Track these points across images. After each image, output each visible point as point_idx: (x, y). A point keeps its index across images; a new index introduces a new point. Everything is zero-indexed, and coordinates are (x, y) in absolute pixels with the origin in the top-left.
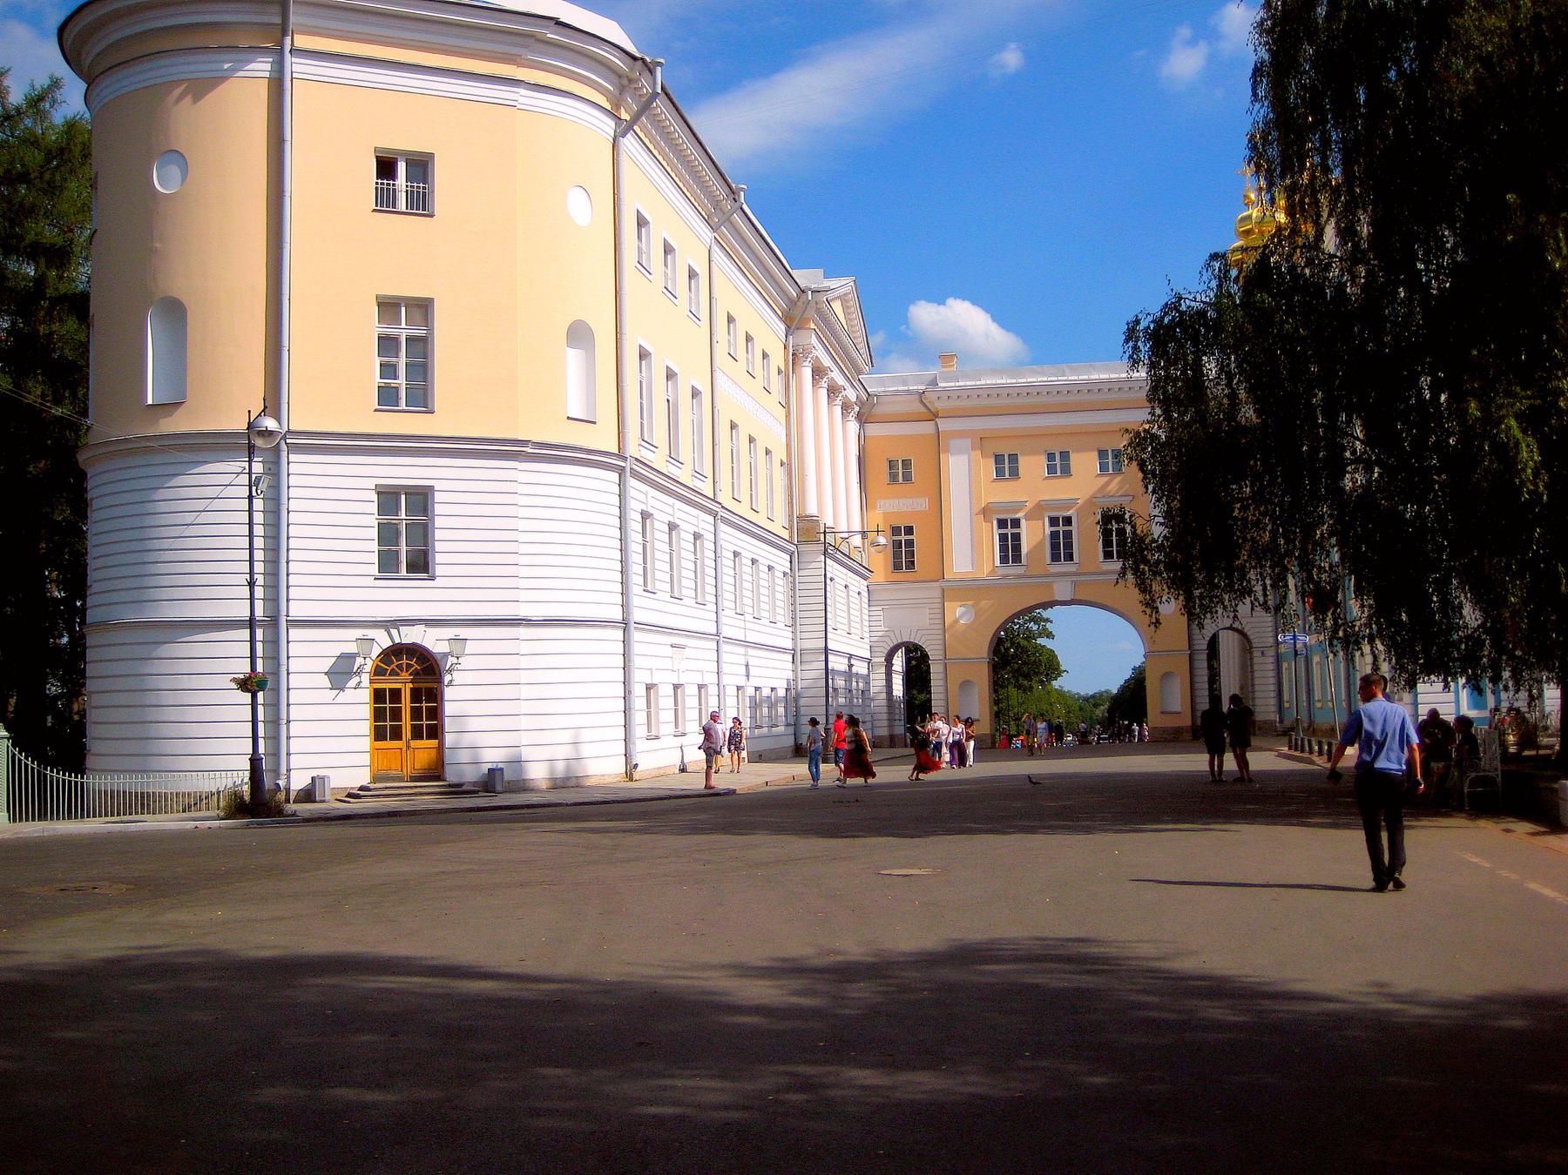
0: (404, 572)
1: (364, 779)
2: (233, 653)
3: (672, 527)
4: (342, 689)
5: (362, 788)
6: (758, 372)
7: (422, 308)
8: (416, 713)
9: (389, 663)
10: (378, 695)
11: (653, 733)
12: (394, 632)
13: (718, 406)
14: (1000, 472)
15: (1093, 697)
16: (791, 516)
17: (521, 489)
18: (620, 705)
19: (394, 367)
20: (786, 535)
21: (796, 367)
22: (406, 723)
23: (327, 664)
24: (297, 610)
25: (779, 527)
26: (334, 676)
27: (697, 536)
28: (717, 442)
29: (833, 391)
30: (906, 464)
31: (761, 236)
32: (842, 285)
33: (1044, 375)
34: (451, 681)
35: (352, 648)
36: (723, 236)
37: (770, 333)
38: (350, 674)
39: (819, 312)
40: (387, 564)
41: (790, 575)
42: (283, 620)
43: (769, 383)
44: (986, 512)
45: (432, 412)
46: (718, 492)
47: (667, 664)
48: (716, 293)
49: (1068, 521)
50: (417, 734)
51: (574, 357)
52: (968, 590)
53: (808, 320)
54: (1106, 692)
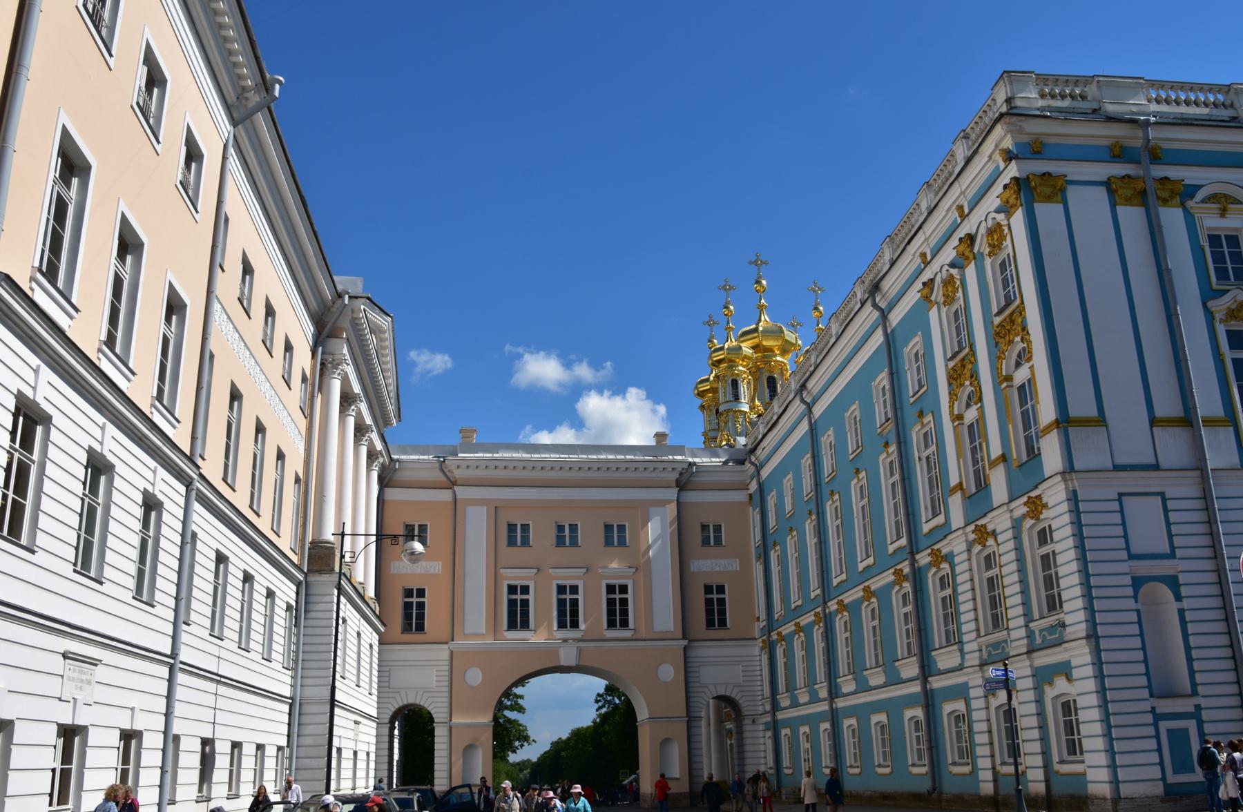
16: (303, 540)
20: (295, 559)
21: (326, 379)
47: (52, 686)
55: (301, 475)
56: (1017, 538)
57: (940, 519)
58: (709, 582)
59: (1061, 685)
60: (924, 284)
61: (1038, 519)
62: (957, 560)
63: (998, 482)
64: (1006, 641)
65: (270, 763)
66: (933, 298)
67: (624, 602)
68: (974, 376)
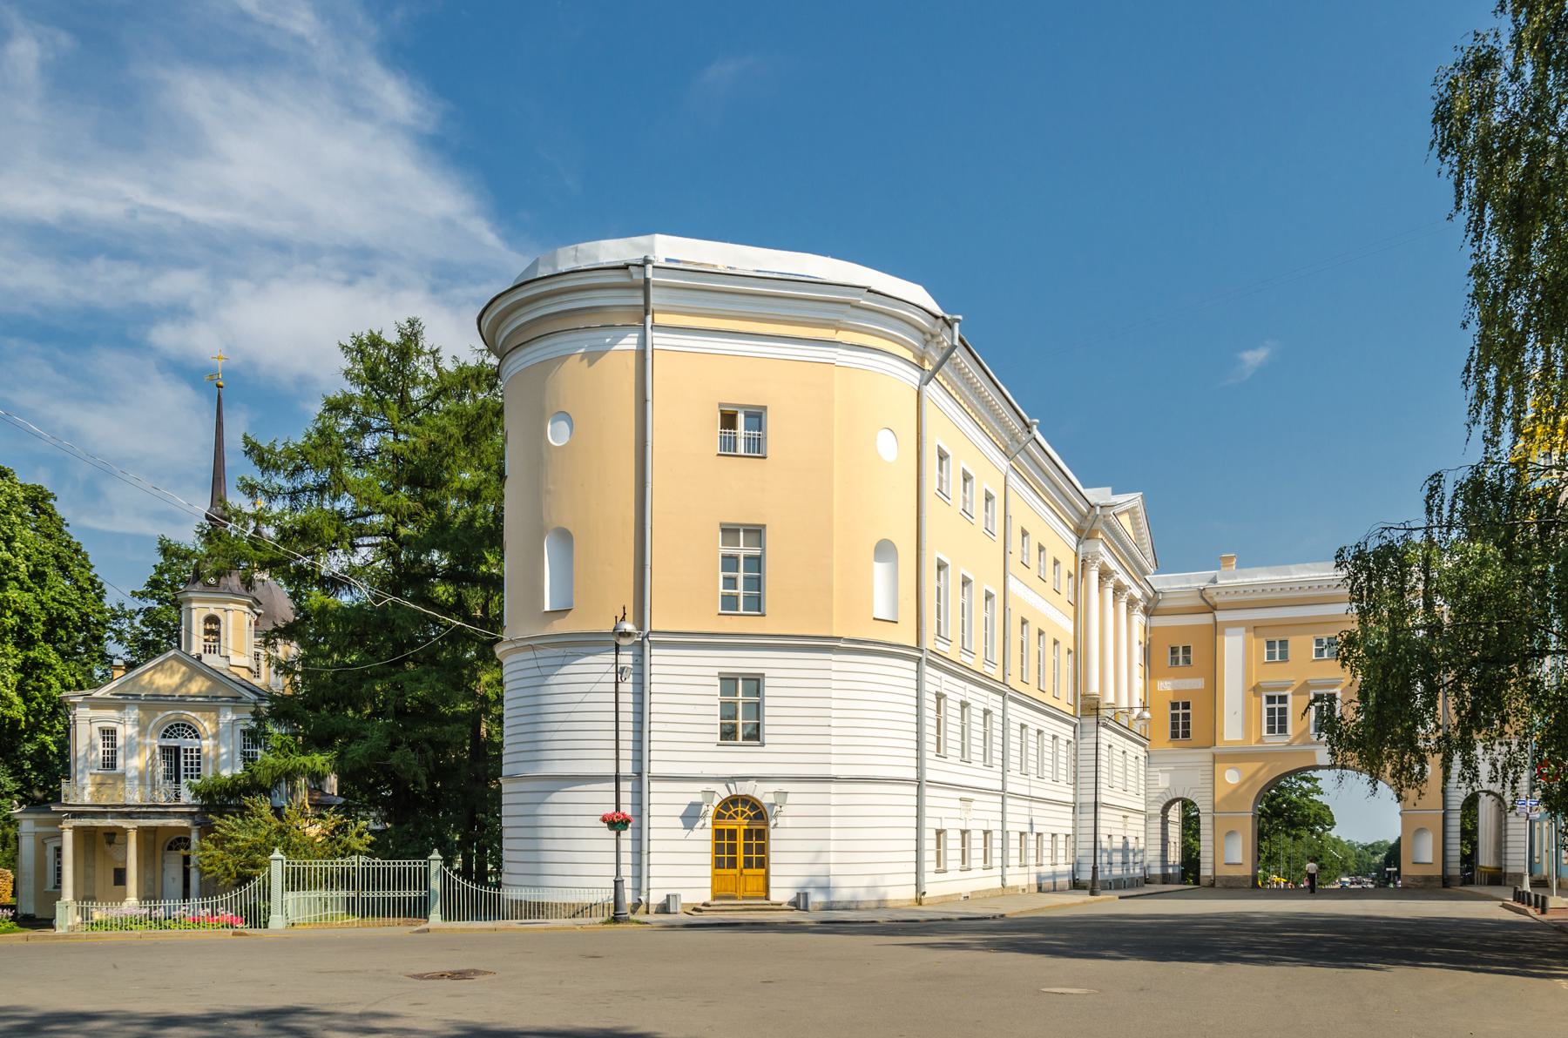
0: (740, 740)
1: (706, 896)
2: (601, 800)
3: (964, 705)
4: (692, 829)
5: (704, 905)
6: (1049, 576)
7: (756, 533)
8: (748, 848)
9: (728, 809)
10: (719, 834)
11: (942, 868)
12: (731, 786)
13: (1010, 605)
14: (1271, 656)
15: (1372, 846)
17: (834, 676)
18: (913, 845)
19: (735, 579)
22: (740, 855)
23: (681, 810)
24: (656, 769)
25: (1065, 704)
26: (685, 819)
27: (987, 712)
28: (1007, 635)
29: (1119, 589)
30: (1187, 650)
31: (1054, 462)
32: (1133, 499)
33: (1318, 571)
34: (776, 825)
35: (698, 798)
36: (1019, 464)
37: (1062, 543)
38: (697, 817)
39: (1108, 525)
40: (728, 734)
41: (1074, 744)
42: (645, 776)
43: (1059, 587)
44: (1257, 690)
45: (764, 615)
46: (1007, 676)
47: (957, 813)
48: (1010, 512)
50: (748, 863)
51: (880, 570)
52: (1236, 757)
53: (1096, 532)
54: (1384, 841)
55: (1072, 649)
65: (1061, 845)
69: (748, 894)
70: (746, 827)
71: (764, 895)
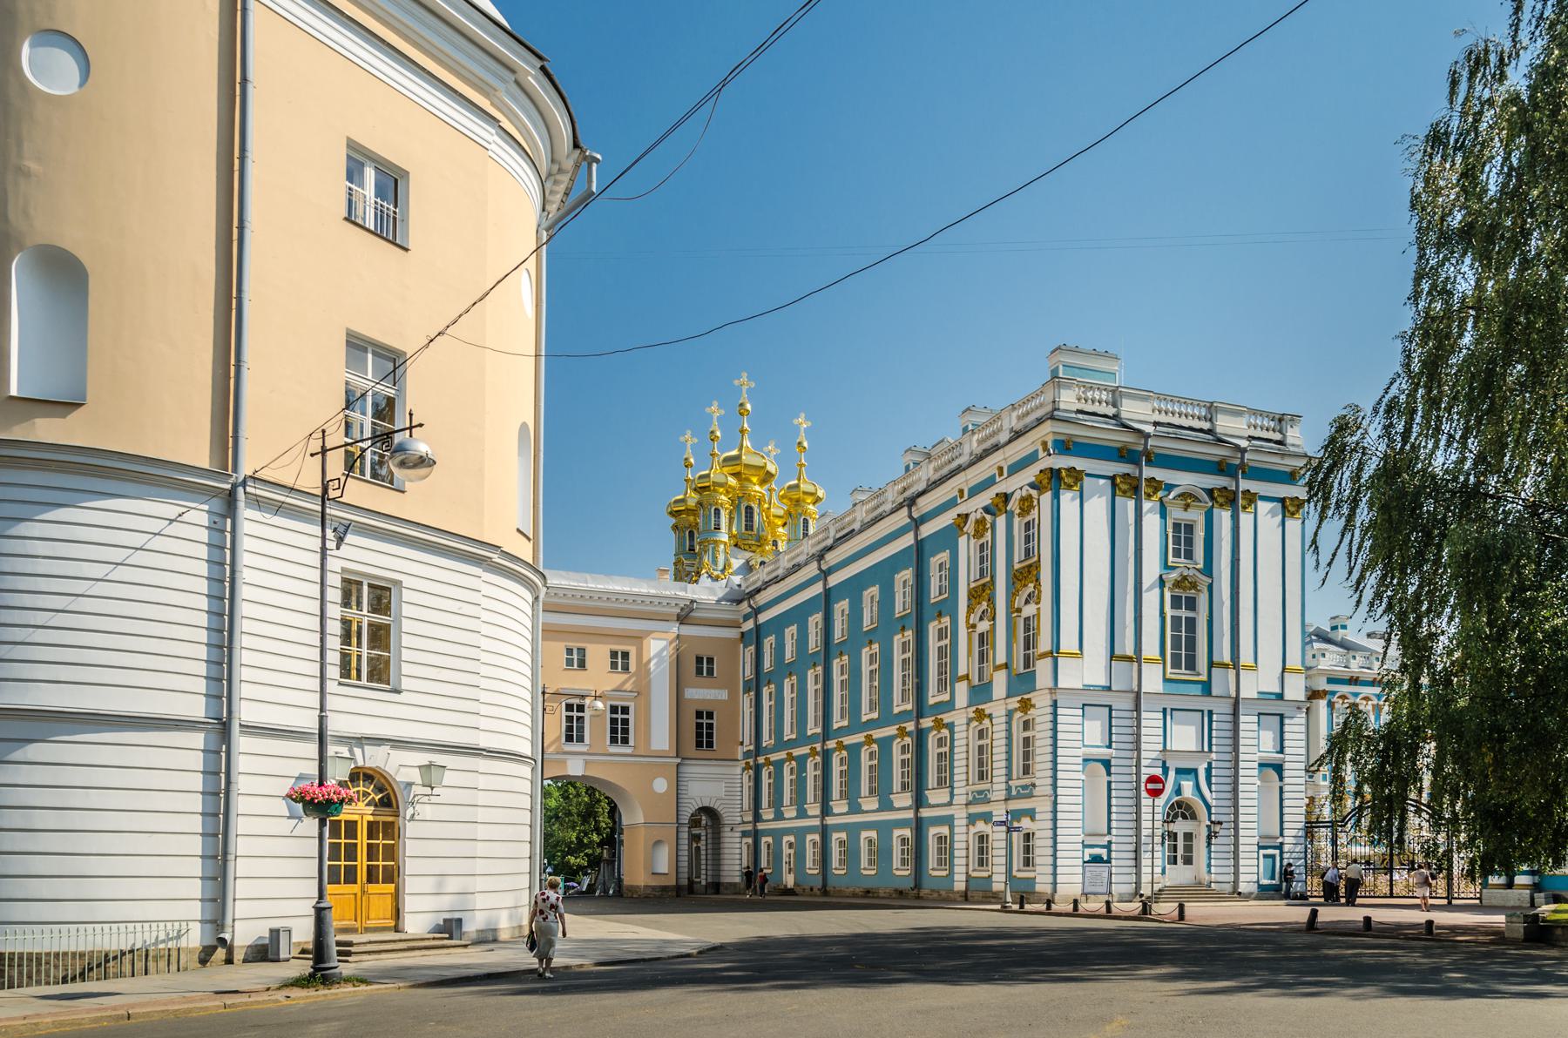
12: (358, 751)
22: (362, 862)
34: (413, 815)
49: (625, 710)
50: (372, 877)
56: (1009, 723)
57: (946, 697)
58: (700, 708)
59: (1025, 823)
60: (959, 515)
61: (1026, 713)
62: (956, 729)
63: (1000, 682)
64: (989, 791)
66: (965, 529)
67: (625, 722)
68: (991, 600)
69: (372, 923)
70: (371, 818)
71: (392, 923)
